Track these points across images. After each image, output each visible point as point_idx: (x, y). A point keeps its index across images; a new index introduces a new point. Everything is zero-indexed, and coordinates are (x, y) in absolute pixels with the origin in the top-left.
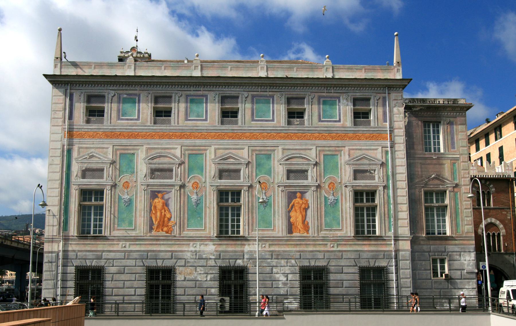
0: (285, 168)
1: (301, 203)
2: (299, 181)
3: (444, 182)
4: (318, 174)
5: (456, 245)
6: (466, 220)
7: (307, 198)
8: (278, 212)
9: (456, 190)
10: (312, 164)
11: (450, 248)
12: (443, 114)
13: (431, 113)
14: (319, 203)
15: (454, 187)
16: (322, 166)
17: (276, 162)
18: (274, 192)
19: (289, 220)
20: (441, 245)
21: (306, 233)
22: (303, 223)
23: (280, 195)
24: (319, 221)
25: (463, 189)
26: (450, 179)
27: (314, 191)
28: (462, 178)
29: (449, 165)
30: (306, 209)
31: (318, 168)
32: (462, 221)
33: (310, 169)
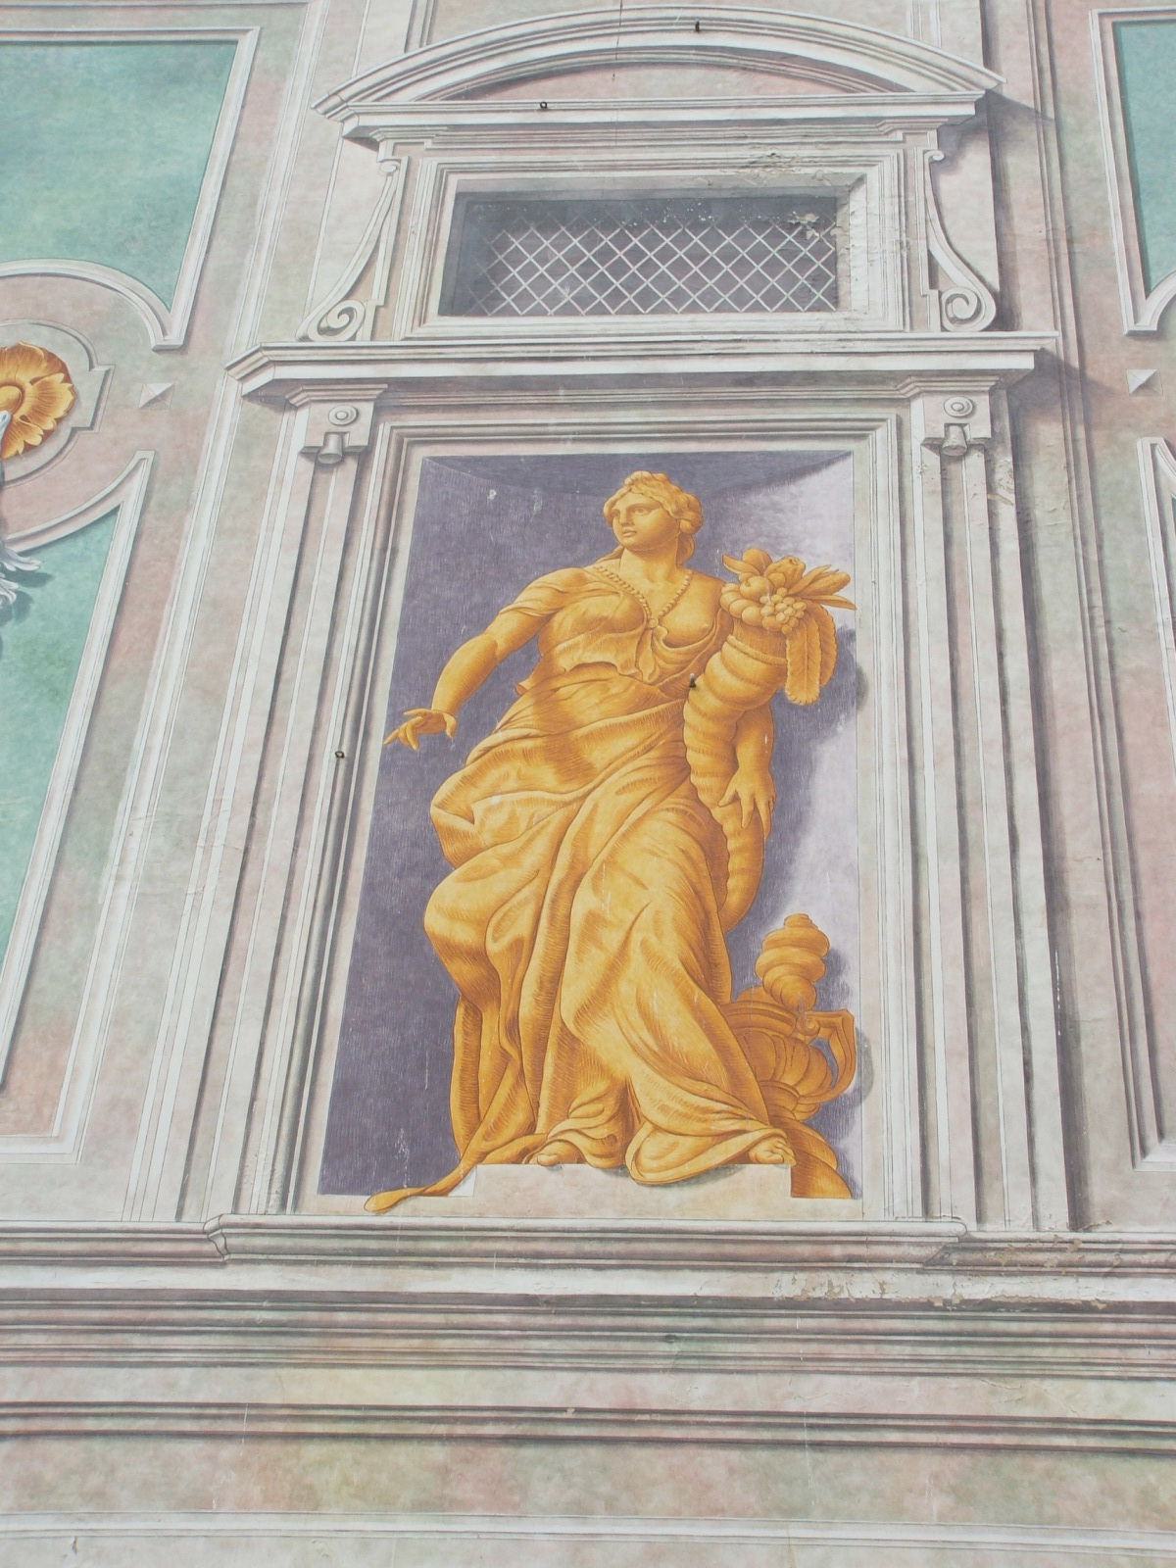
0: (432, 184)
1: (690, 617)
2: (679, 323)
4: (1029, 228)
7: (818, 554)
8: (187, 776)
10: (913, 127)
14: (1062, 614)
16: (1099, 141)
17: (293, 115)
18: (172, 476)
19: (394, 925)
21: (780, 1176)
22: (704, 971)
23: (282, 512)
24: (1088, 927)
27: (948, 455)
30: (783, 730)
31: (1022, 165)
33: (880, 179)
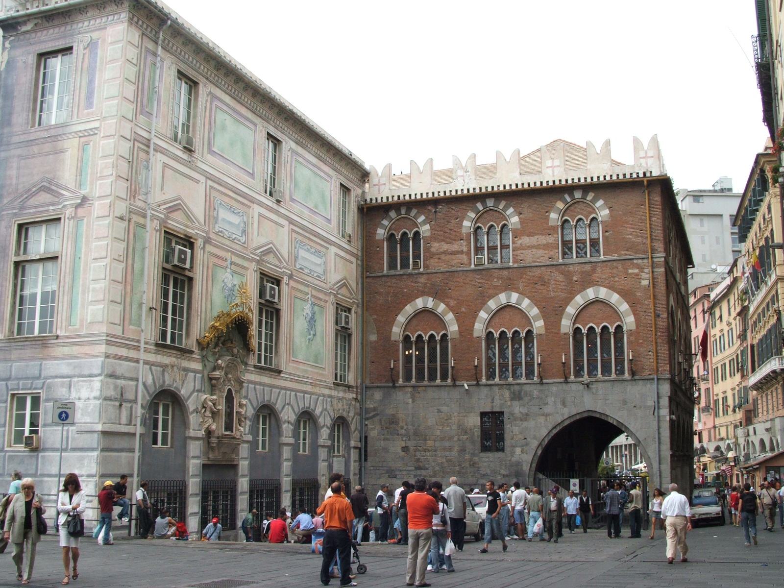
3: (58, 195)
5: (64, 358)
6: (94, 290)
9: (81, 212)
11: (54, 367)
12: (80, 25)
13: (57, 30)
15: (78, 206)
20: (32, 359)
25: (98, 207)
26: (72, 185)
28: (97, 179)
29: (76, 151)
32: (84, 293)
